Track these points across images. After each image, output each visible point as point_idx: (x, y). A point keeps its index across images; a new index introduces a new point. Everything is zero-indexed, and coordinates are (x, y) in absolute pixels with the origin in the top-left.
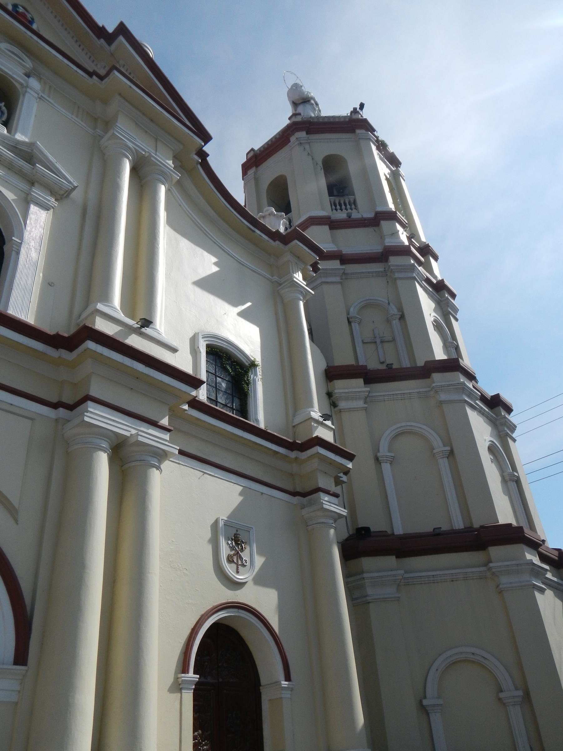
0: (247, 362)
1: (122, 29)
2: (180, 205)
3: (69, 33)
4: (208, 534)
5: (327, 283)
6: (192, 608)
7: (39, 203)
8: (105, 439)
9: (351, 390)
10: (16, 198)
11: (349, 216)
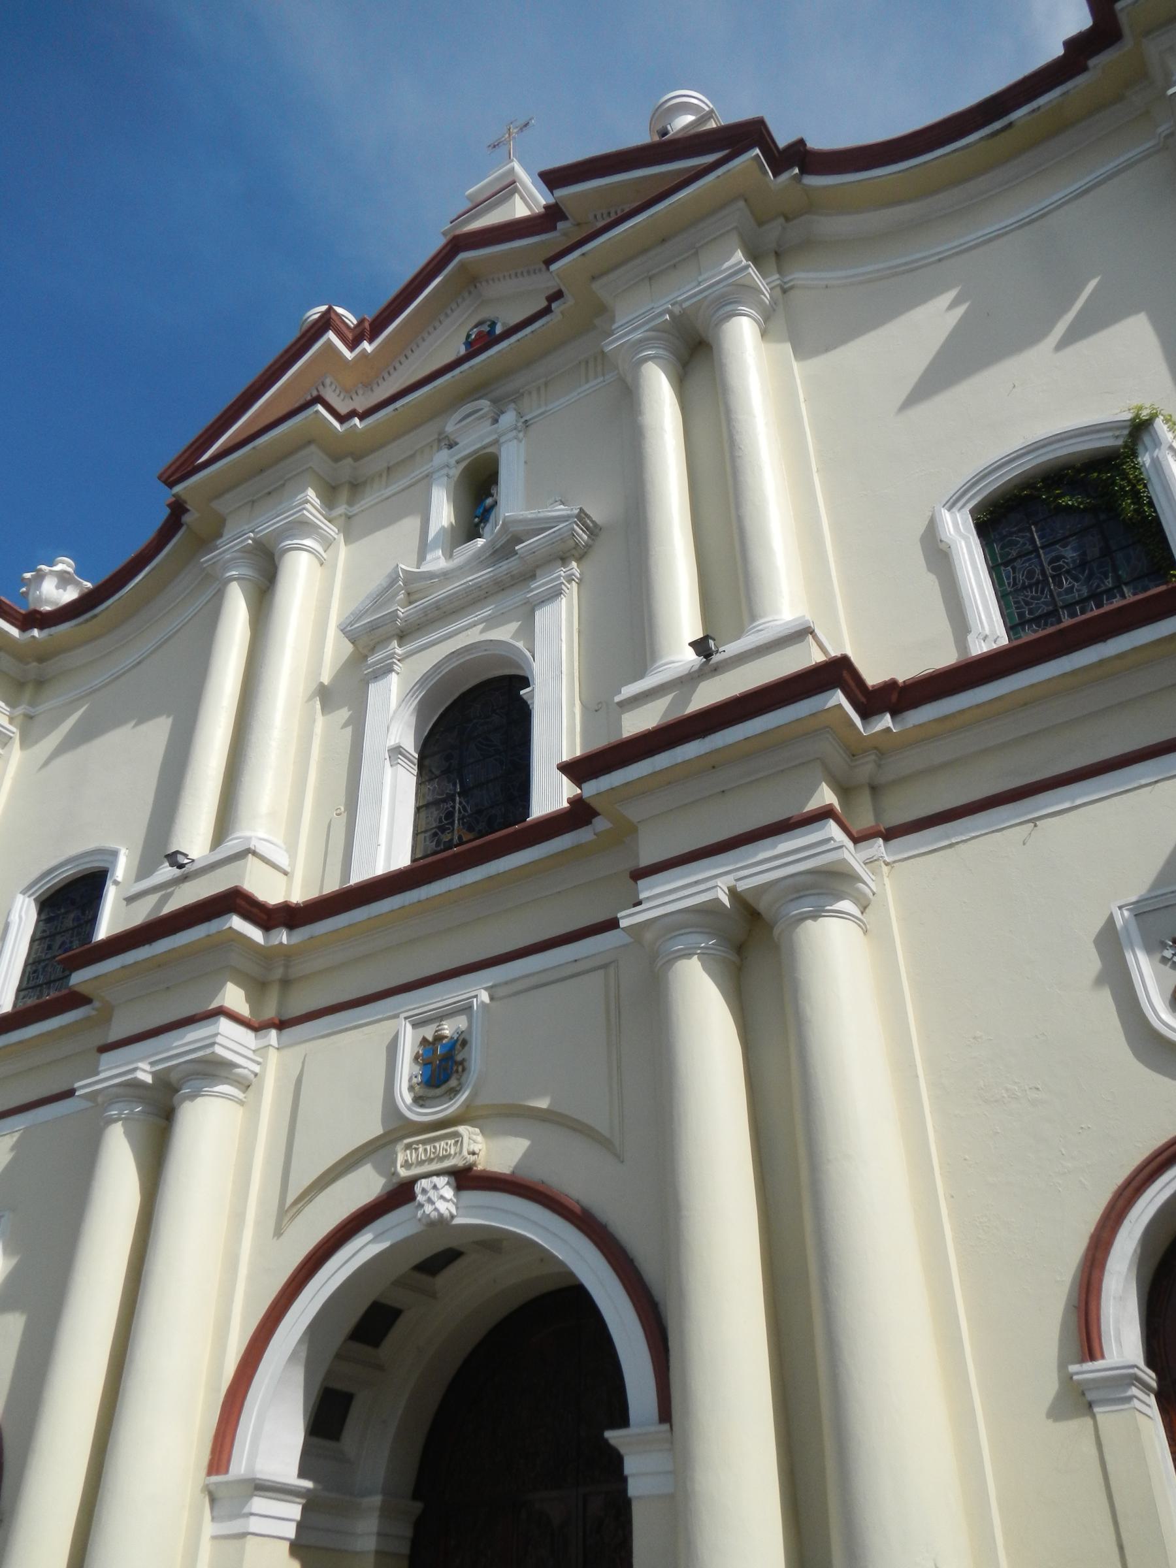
0: (1117, 437)
1: (552, 179)
4: (1093, 963)
6: (1080, 1181)
7: (543, 599)
8: (683, 931)
10: (520, 623)
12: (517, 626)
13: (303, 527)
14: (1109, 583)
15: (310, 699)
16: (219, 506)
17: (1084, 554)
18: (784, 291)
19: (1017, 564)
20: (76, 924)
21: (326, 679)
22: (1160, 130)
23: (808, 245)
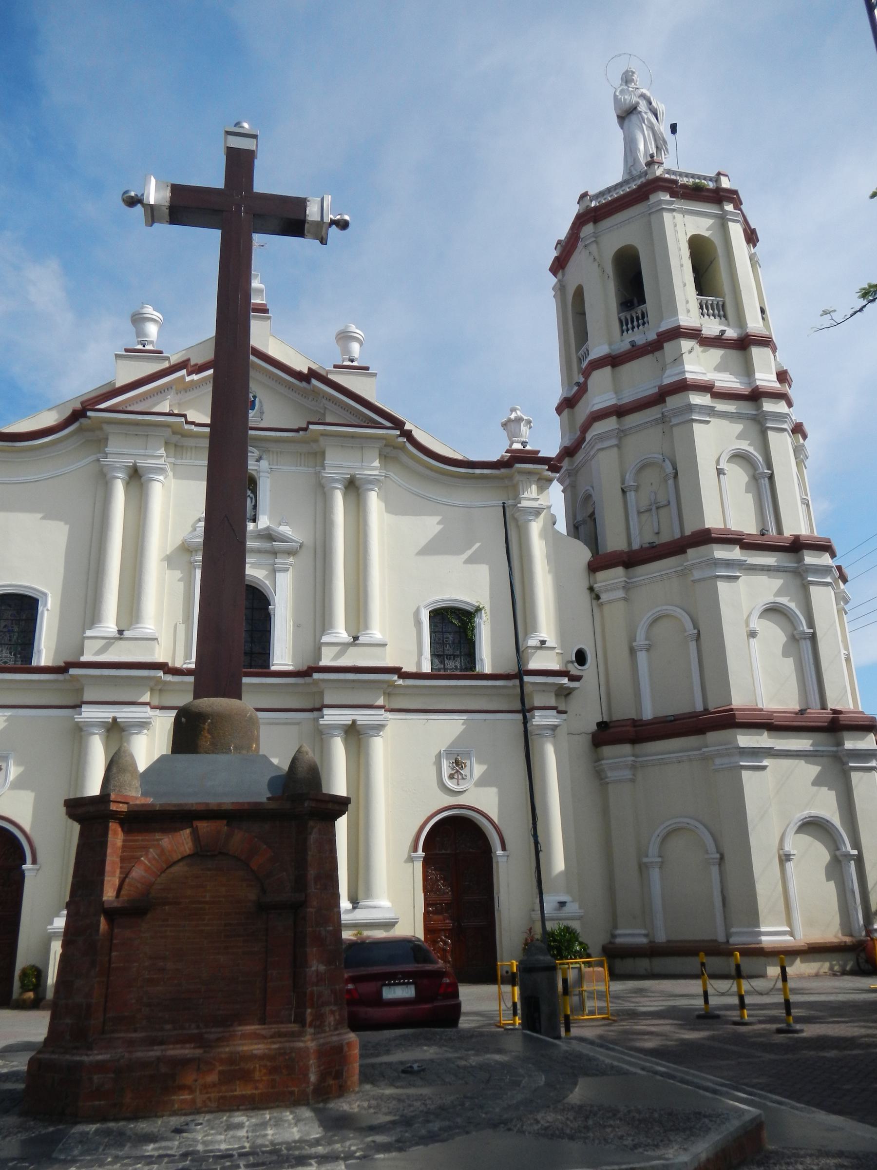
2: (400, 486)
3: (282, 385)
5: (603, 449)
9: (607, 583)
11: (633, 344)
12: (338, 650)
13: (161, 470)
14: (458, 653)
15: (163, 560)
16: (105, 427)
17: (454, 640)
18: (385, 477)
19: (437, 634)
20: (13, 618)
21: (168, 552)
22: (509, 501)
23: (395, 459)
